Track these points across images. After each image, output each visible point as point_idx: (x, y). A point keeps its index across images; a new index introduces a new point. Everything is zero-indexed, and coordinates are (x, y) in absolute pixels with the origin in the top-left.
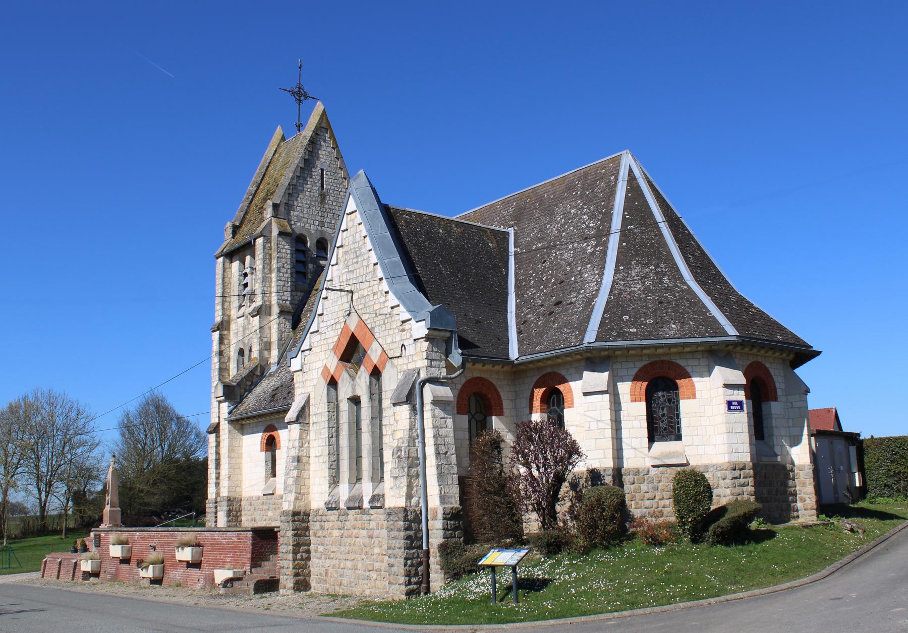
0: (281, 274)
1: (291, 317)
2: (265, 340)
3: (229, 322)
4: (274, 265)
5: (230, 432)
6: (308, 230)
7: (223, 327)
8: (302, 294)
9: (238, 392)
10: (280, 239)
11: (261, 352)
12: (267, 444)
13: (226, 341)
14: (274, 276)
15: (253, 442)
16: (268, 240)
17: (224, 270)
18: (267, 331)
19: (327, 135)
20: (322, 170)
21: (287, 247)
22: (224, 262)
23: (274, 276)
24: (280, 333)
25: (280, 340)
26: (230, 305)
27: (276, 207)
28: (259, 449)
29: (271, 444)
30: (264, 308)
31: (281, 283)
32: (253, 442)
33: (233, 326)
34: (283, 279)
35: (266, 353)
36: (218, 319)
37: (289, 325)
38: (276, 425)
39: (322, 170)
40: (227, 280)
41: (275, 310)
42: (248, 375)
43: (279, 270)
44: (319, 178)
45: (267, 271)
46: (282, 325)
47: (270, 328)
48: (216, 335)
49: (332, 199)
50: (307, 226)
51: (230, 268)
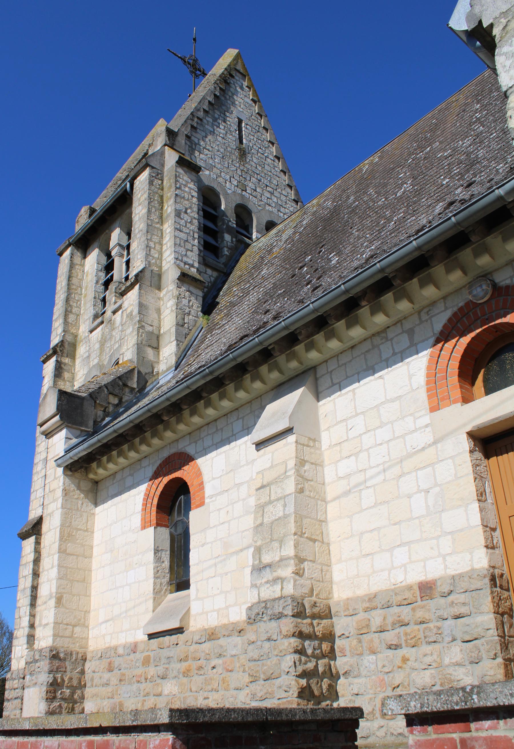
0: (182, 222)
1: (201, 294)
2: (149, 328)
3: (74, 346)
4: (169, 208)
5: (66, 492)
6: (224, 188)
7: (65, 350)
8: (215, 274)
9: (93, 412)
10: (180, 170)
11: (140, 348)
12: (159, 507)
13: (66, 375)
14: (168, 228)
15: (125, 517)
16: (158, 175)
17: (72, 266)
18: (152, 315)
19: (245, 84)
20: (240, 121)
21: (191, 185)
22: (72, 256)
23: (168, 228)
24: (182, 315)
25: (180, 325)
26: (77, 319)
27: (171, 134)
28: (137, 520)
29: (174, 503)
30: (147, 274)
31: (183, 236)
32: (125, 517)
33: (81, 350)
34: (185, 230)
35: (150, 353)
36: (55, 340)
37: (196, 305)
38: (191, 450)
39: (240, 121)
40: (74, 281)
41: (171, 274)
42: (113, 383)
43: (178, 214)
44: (236, 127)
45: (154, 217)
46: (185, 302)
47: (158, 311)
48: (50, 366)
49: (255, 160)
50: (220, 180)
51: (83, 265)
